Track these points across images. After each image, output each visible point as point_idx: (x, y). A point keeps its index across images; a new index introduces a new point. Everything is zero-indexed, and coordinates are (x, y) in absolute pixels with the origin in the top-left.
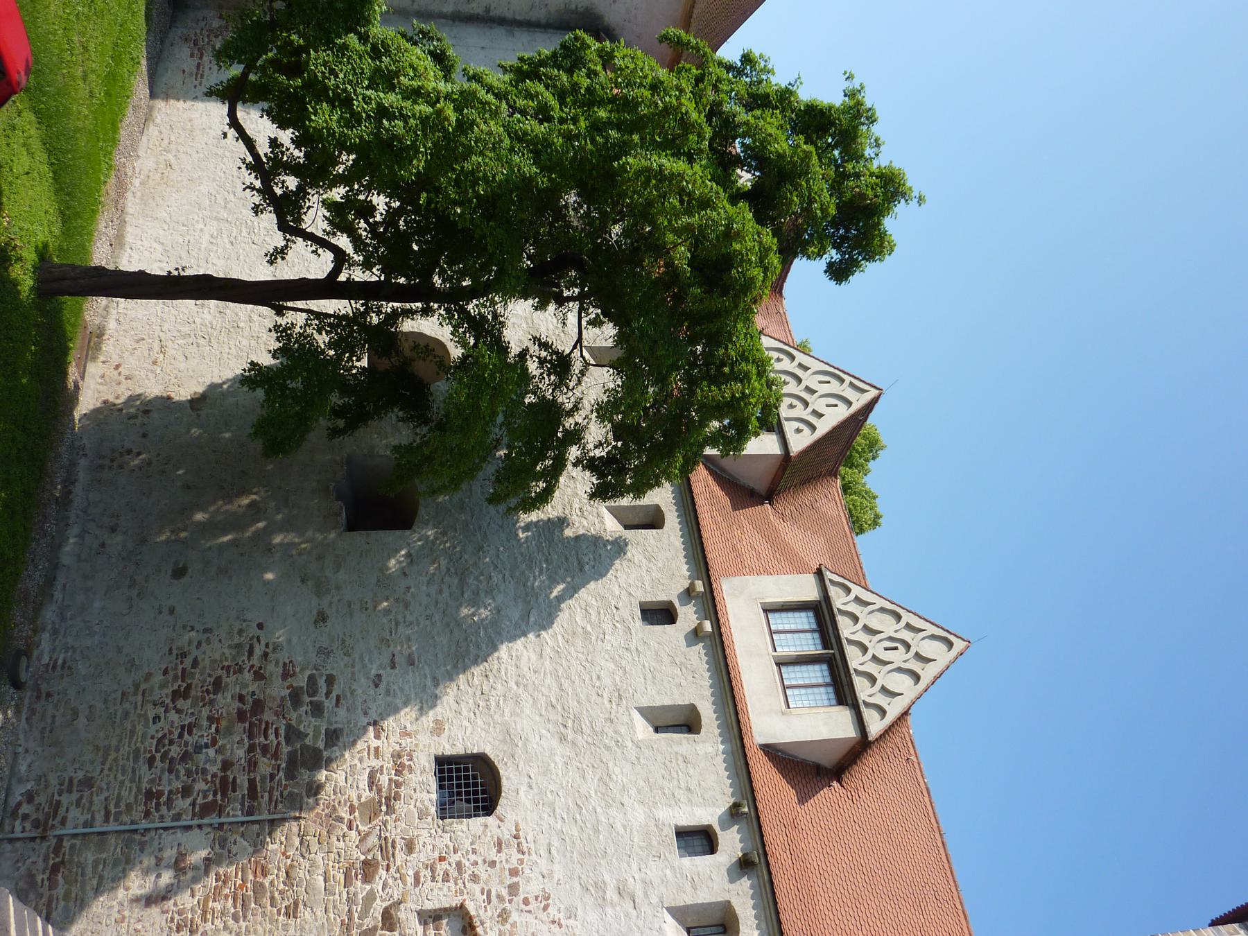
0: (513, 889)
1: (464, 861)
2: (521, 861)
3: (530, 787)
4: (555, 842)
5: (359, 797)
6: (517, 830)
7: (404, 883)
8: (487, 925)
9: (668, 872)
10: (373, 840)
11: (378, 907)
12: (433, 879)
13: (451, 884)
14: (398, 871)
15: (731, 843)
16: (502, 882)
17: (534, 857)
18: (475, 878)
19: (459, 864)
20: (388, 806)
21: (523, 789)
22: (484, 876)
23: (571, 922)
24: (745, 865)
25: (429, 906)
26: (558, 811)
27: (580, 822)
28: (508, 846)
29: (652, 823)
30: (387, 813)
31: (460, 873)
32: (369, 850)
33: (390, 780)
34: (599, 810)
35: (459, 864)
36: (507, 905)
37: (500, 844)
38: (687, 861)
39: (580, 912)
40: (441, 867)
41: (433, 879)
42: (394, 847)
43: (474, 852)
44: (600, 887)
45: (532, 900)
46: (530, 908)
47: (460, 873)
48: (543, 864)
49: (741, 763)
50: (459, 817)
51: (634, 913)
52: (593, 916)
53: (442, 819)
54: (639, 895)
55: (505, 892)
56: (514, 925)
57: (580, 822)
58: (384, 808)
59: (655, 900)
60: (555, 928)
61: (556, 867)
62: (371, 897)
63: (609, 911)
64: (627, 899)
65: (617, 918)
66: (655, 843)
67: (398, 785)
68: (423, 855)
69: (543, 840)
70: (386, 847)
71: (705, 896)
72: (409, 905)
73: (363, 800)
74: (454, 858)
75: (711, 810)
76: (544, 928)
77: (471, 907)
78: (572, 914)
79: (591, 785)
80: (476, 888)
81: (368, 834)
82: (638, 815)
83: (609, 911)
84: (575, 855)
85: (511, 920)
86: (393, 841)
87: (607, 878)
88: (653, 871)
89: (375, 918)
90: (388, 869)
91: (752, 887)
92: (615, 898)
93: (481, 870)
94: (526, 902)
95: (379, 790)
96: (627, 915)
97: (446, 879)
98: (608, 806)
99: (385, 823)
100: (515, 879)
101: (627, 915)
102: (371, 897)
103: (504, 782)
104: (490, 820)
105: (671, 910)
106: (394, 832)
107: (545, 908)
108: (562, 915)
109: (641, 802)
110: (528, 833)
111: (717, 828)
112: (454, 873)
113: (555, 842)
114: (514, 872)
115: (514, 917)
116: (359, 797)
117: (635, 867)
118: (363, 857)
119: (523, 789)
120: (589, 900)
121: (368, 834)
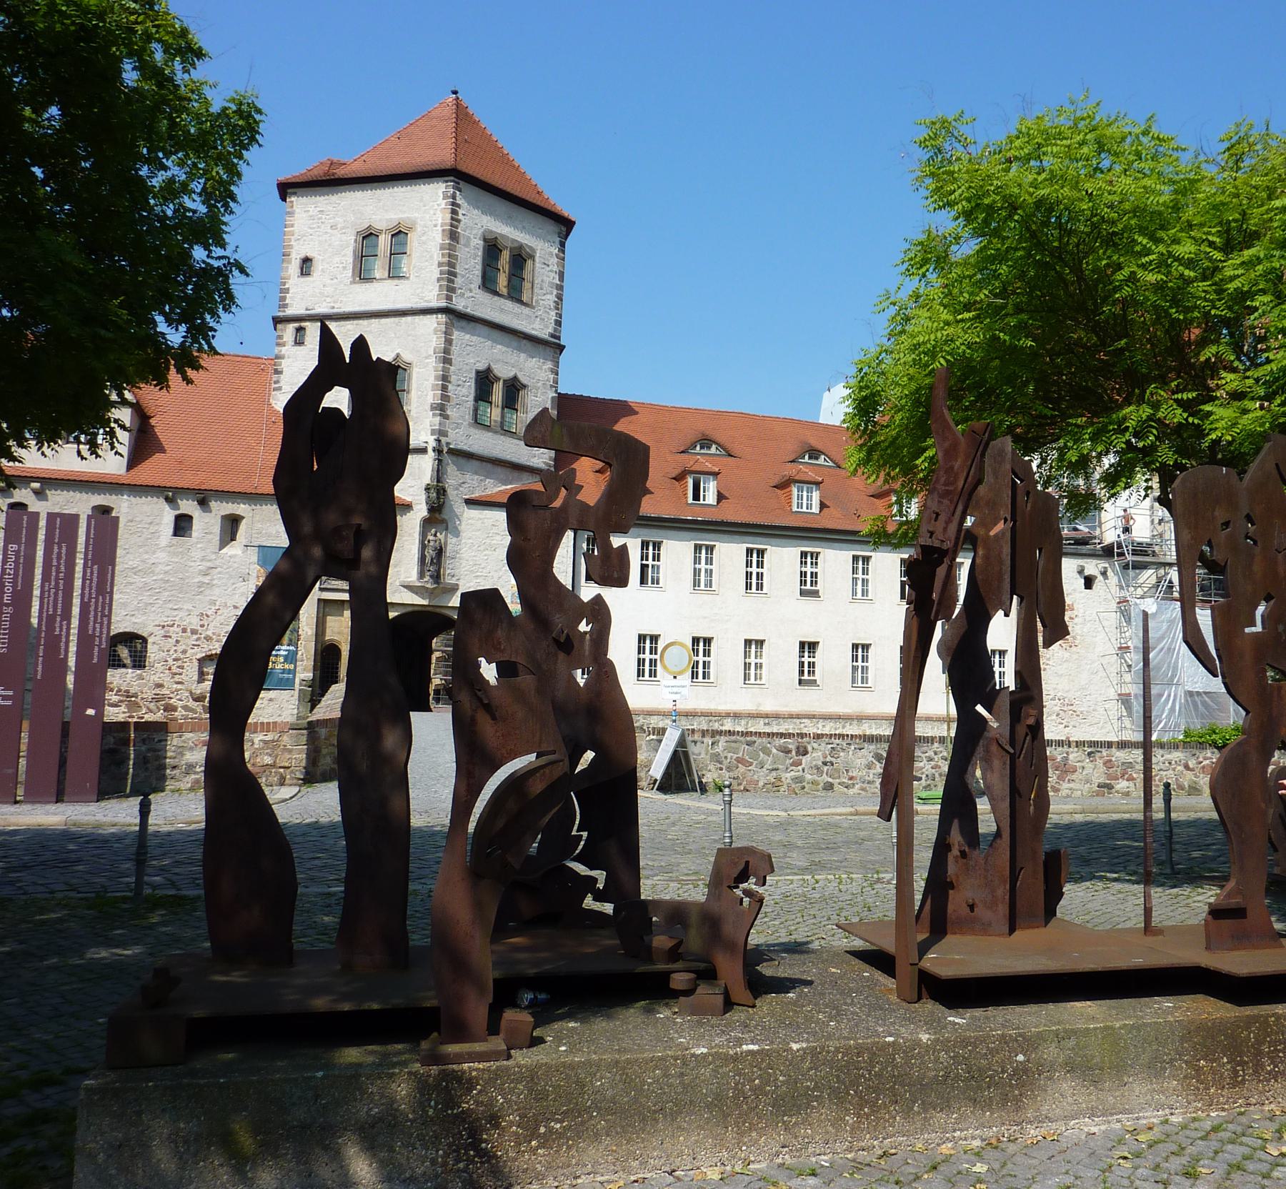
0: (194, 632)
1: (173, 657)
2: (178, 625)
3: (133, 615)
4: (170, 606)
5: (124, 713)
6: (159, 626)
7: (181, 689)
8: (212, 648)
9: (199, 546)
10: (152, 706)
11: (191, 704)
12: (181, 674)
13: (185, 665)
14: (173, 693)
15: (188, 506)
16: (189, 638)
17: (177, 618)
18: (184, 652)
19: (174, 660)
20: (132, 697)
21: (134, 619)
22: (184, 647)
23: (217, 603)
24: (203, 503)
25: (196, 677)
26: (151, 601)
27: (160, 590)
28: (168, 632)
29: (169, 549)
30: (137, 697)
31: (180, 659)
32: (158, 708)
33: (115, 695)
34: (154, 578)
35: (174, 660)
36: (202, 636)
37: (166, 636)
38: (194, 534)
39: (212, 598)
40: (174, 669)
41: (181, 674)
42: (158, 695)
43: (168, 651)
44: (201, 584)
45: (202, 622)
46: (206, 624)
47: (180, 659)
48: (181, 614)
49: (139, 489)
50: (145, 656)
51: (219, 569)
52: (217, 591)
53: (145, 667)
54: (209, 564)
55: (195, 637)
56: (214, 634)
57: (160, 590)
58: (133, 699)
59: (213, 557)
60: (219, 612)
61: (185, 607)
62: (185, 708)
63: (214, 582)
64: (210, 571)
65: (219, 578)
66: (181, 550)
67: (119, 690)
68: (166, 679)
69: (168, 612)
70: (157, 699)
71: (217, 529)
72: (193, 687)
73: (126, 710)
74: (171, 662)
75: (166, 513)
76: (218, 618)
77: (200, 656)
78: (213, 603)
79: (137, 579)
80: (190, 651)
81: (148, 708)
82: (162, 556)
83: (214, 582)
84: (180, 596)
85: (211, 635)
86: (155, 694)
87: (196, 580)
88: (196, 554)
89: (198, 706)
90: (171, 698)
91: (216, 501)
92: (209, 577)
93: (180, 648)
94: (202, 626)
95: (121, 701)
96: (220, 573)
97: (182, 668)
98: (153, 572)
99: (142, 699)
100: (189, 630)
101: (220, 573)
102: (185, 708)
103: (127, 630)
104: (150, 640)
105: (221, 548)
106: (149, 694)
107: (208, 616)
108: (213, 608)
109: (154, 553)
110: (162, 620)
111: (178, 512)
112: (179, 663)
113: (170, 606)
114: (184, 631)
115: (209, 633)
116: (124, 713)
117: (193, 564)
118: (162, 711)
119: (134, 619)
120: (207, 592)
121: (148, 708)
